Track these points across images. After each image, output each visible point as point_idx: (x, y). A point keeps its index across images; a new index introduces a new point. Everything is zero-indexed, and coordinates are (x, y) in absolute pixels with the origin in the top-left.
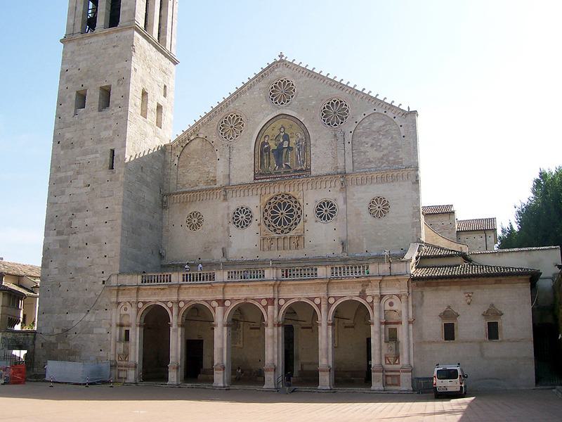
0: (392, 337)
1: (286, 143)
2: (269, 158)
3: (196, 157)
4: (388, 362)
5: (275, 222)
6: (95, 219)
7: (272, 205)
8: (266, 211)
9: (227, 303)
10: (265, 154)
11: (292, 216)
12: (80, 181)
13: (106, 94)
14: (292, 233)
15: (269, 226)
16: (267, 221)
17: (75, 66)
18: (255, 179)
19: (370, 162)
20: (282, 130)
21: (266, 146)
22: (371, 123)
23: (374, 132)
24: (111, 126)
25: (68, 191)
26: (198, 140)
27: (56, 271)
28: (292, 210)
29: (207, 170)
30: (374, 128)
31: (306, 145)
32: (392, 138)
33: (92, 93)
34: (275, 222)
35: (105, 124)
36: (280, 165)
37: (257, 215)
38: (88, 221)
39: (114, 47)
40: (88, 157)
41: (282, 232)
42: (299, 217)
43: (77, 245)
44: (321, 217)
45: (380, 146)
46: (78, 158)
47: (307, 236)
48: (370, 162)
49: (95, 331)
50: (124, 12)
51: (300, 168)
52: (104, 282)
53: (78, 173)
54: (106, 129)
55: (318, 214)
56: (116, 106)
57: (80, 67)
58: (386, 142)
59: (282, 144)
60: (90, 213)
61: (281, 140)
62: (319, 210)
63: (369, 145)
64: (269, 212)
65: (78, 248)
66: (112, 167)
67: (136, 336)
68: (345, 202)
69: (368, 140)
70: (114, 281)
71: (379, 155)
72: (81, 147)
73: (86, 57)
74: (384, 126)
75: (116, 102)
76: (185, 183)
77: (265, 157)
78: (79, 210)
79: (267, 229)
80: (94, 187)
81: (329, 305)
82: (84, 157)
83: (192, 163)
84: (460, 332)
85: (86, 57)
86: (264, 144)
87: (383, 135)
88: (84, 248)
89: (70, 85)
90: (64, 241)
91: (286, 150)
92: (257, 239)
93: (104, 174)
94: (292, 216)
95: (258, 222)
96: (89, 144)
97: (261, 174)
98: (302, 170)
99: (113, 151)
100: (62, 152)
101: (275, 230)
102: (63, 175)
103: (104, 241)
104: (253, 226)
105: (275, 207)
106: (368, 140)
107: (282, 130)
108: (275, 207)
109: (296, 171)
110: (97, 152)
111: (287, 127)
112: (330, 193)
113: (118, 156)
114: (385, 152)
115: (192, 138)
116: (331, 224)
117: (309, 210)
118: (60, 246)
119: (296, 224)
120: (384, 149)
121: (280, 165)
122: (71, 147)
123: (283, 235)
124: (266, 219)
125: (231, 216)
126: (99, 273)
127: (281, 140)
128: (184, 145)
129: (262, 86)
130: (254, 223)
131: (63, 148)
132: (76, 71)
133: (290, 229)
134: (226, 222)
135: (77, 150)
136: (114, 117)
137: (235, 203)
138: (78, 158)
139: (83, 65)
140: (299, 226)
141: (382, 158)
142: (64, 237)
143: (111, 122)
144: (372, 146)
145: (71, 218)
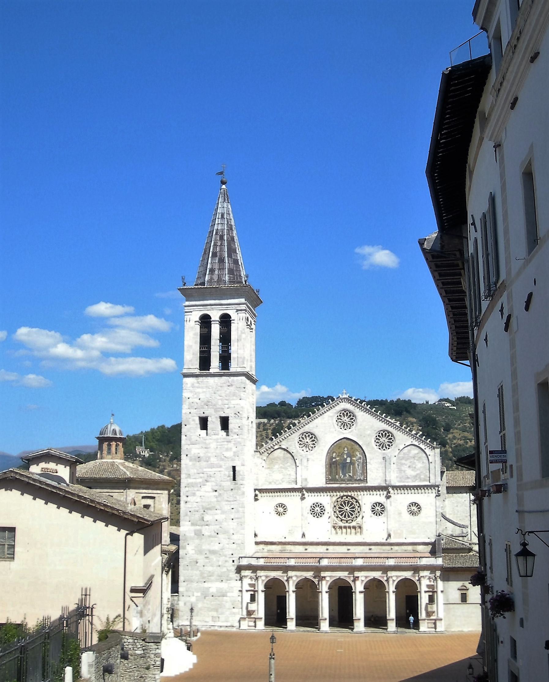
0: (431, 600)
1: (348, 460)
2: (337, 469)
3: (279, 462)
4: (428, 615)
5: (341, 515)
6: (223, 516)
7: (339, 503)
8: (335, 506)
9: (328, 579)
10: (333, 465)
11: (354, 511)
12: (208, 487)
13: (225, 423)
14: (354, 524)
15: (337, 517)
16: (335, 514)
17: (195, 396)
18: (326, 483)
19: (408, 478)
20: (346, 449)
21: (334, 460)
22: (409, 451)
23: (411, 457)
24: (231, 449)
25: (198, 494)
26: (280, 450)
27: (193, 552)
28: (354, 508)
29: (289, 473)
30: (411, 455)
31: (363, 463)
32: (423, 462)
33: (214, 420)
34: (341, 515)
35: (226, 446)
36: (345, 475)
37: (329, 509)
38: (217, 517)
39: (229, 386)
40: (214, 469)
41: (347, 522)
42: (359, 512)
43: (209, 534)
44: (374, 514)
45: (415, 467)
46: (205, 470)
47: (364, 527)
48: (408, 478)
49: (229, 594)
50: (234, 358)
51: (359, 478)
52: (233, 561)
53: (207, 481)
54: (227, 450)
55: (372, 511)
56: (235, 433)
57: (201, 397)
58: (419, 465)
59: (346, 459)
60: (218, 512)
61: (345, 457)
62: (373, 508)
63: (408, 466)
64: (337, 508)
65: (210, 536)
66: (234, 479)
67: (261, 597)
68: (391, 505)
69: (406, 462)
70: (244, 562)
71: (413, 473)
72: (207, 461)
73: (204, 390)
74: (418, 454)
75: (235, 431)
76: (271, 481)
77: (333, 468)
78: (208, 509)
79: (335, 519)
80: (220, 492)
81: (394, 581)
82: (210, 470)
83: (277, 466)
84: (470, 599)
85: (204, 390)
86: (332, 458)
87: (417, 460)
88: (215, 537)
89: (193, 411)
90: (198, 530)
91: (349, 464)
92: (329, 526)
93: (229, 483)
94: (354, 511)
95: (329, 515)
96: (213, 460)
97: (330, 480)
98: (360, 480)
99: (234, 468)
100: (191, 463)
101: (341, 521)
102: (193, 481)
103: (232, 532)
104: (326, 516)
105: (341, 505)
106: (406, 462)
107: (346, 449)
108: (341, 505)
109: (356, 480)
110: (221, 467)
111: (349, 447)
112: (380, 497)
113: (239, 471)
114: (418, 472)
115: (276, 447)
116: (382, 518)
117: (366, 508)
118: (195, 534)
119: (356, 517)
120: (417, 470)
121: (345, 475)
122: (198, 460)
123: (347, 525)
124: (335, 512)
125: (309, 508)
126: (229, 555)
127: (345, 457)
128: (269, 452)
129: (331, 415)
130: (326, 512)
131: (191, 460)
132: (198, 401)
133: (352, 521)
134: (305, 514)
135: (203, 464)
136: (233, 442)
137: (311, 499)
138: (205, 470)
139: (202, 396)
140: (359, 519)
141: (416, 476)
142: (198, 528)
143: (231, 445)
144: (409, 467)
145: (203, 514)
